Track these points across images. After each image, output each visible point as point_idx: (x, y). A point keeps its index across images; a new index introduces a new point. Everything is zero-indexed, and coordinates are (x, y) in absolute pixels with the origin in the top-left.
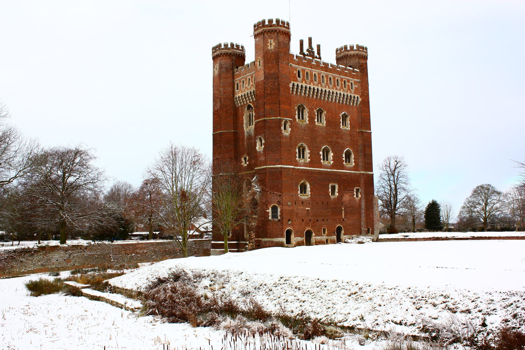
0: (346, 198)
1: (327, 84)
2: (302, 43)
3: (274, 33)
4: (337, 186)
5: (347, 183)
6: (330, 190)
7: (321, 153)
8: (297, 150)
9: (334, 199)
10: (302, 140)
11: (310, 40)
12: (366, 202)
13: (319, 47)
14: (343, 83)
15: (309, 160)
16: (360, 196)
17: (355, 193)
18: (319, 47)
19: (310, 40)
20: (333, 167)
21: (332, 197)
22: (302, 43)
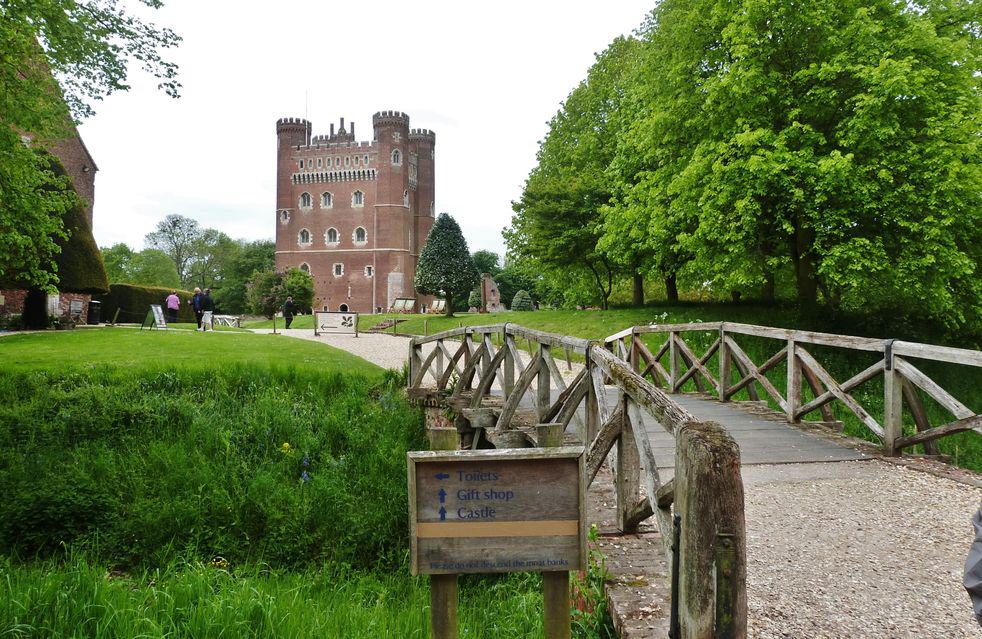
0: (354, 277)
1: (333, 166)
2: (332, 126)
3: (292, 133)
4: (342, 267)
5: (356, 262)
6: (334, 270)
7: (326, 235)
8: (299, 236)
9: (339, 279)
10: (305, 224)
11: (342, 120)
12: (377, 278)
13: (352, 124)
14: (354, 160)
15: (310, 243)
16: (372, 274)
17: (366, 271)
18: (352, 124)
19: (342, 120)
20: (339, 247)
21: (336, 276)
22: (332, 126)
